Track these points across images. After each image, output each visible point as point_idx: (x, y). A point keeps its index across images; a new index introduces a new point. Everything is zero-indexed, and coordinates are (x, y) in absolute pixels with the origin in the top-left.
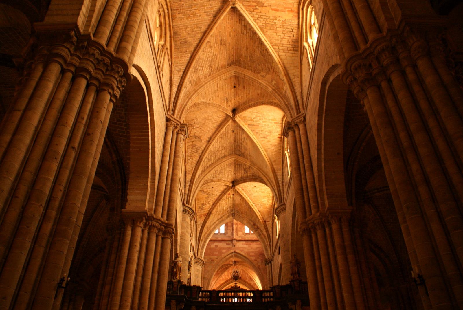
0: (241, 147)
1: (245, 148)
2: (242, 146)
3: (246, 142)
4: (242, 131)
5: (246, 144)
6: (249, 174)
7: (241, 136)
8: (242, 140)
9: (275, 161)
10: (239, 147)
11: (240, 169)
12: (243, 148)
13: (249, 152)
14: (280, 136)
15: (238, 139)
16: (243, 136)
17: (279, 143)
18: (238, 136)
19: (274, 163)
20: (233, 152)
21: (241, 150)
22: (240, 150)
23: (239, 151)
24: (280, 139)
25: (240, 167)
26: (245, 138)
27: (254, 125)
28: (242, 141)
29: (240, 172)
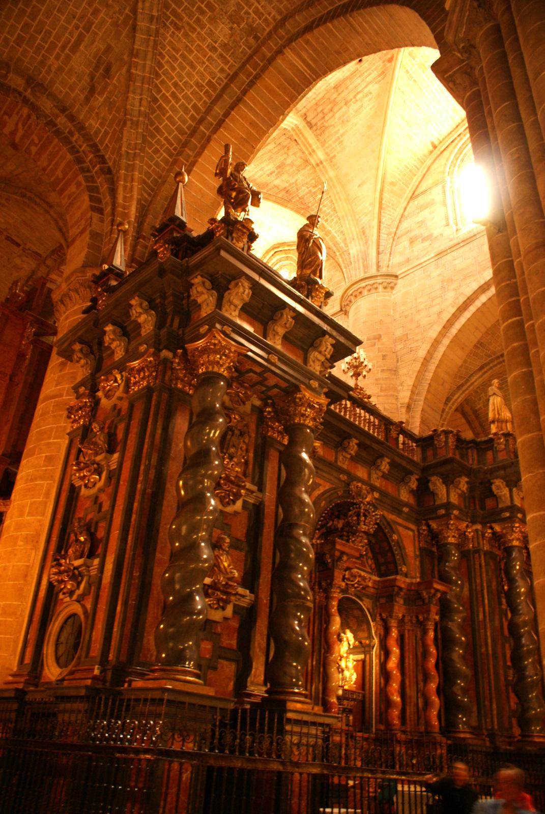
0: (335, 110)
1: (345, 118)
2: (345, 109)
3: (362, 106)
4: (380, 75)
5: (357, 112)
6: (277, 182)
7: (364, 85)
8: (358, 93)
9: (392, 184)
10: (330, 107)
11: (270, 158)
12: (337, 116)
13: (346, 131)
14: (436, 143)
15: (351, 87)
16: (370, 86)
17: (424, 155)
18: (359, 81)
19: (387, 187)
20: (304, 110)
21: (327, 118)
22: (325, 115)
23: (321, 115)
24: (431, 148)
25: (278, 152)
26: (370, 96)
27: (415, 81)
28: (355, 97)
29: (263, 165)
